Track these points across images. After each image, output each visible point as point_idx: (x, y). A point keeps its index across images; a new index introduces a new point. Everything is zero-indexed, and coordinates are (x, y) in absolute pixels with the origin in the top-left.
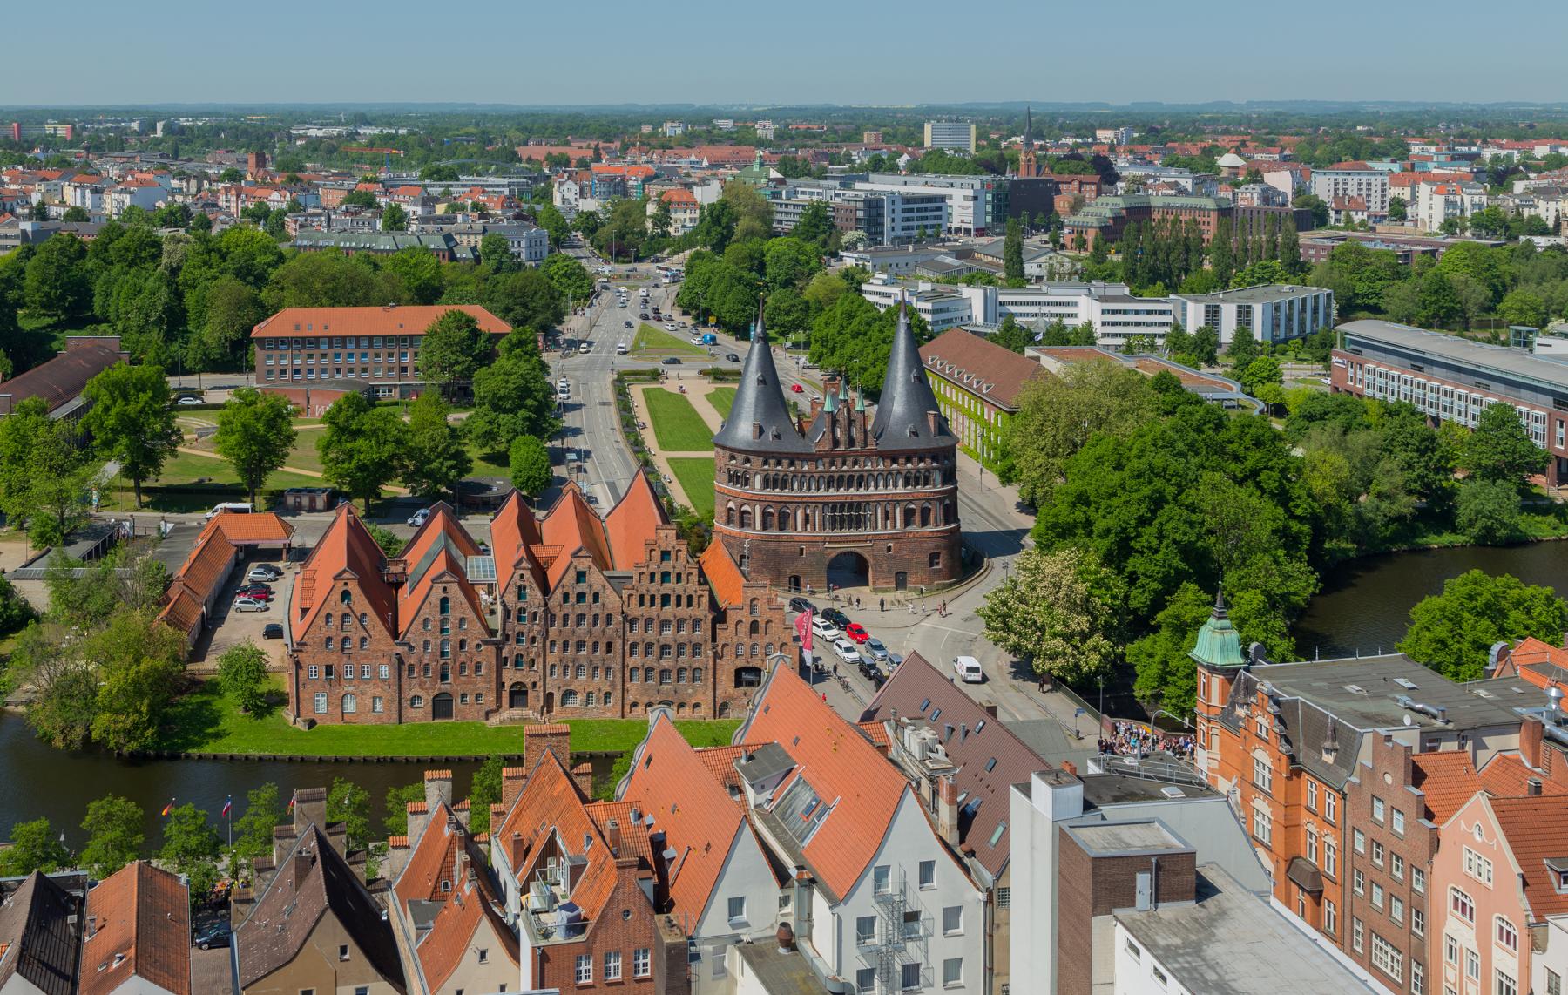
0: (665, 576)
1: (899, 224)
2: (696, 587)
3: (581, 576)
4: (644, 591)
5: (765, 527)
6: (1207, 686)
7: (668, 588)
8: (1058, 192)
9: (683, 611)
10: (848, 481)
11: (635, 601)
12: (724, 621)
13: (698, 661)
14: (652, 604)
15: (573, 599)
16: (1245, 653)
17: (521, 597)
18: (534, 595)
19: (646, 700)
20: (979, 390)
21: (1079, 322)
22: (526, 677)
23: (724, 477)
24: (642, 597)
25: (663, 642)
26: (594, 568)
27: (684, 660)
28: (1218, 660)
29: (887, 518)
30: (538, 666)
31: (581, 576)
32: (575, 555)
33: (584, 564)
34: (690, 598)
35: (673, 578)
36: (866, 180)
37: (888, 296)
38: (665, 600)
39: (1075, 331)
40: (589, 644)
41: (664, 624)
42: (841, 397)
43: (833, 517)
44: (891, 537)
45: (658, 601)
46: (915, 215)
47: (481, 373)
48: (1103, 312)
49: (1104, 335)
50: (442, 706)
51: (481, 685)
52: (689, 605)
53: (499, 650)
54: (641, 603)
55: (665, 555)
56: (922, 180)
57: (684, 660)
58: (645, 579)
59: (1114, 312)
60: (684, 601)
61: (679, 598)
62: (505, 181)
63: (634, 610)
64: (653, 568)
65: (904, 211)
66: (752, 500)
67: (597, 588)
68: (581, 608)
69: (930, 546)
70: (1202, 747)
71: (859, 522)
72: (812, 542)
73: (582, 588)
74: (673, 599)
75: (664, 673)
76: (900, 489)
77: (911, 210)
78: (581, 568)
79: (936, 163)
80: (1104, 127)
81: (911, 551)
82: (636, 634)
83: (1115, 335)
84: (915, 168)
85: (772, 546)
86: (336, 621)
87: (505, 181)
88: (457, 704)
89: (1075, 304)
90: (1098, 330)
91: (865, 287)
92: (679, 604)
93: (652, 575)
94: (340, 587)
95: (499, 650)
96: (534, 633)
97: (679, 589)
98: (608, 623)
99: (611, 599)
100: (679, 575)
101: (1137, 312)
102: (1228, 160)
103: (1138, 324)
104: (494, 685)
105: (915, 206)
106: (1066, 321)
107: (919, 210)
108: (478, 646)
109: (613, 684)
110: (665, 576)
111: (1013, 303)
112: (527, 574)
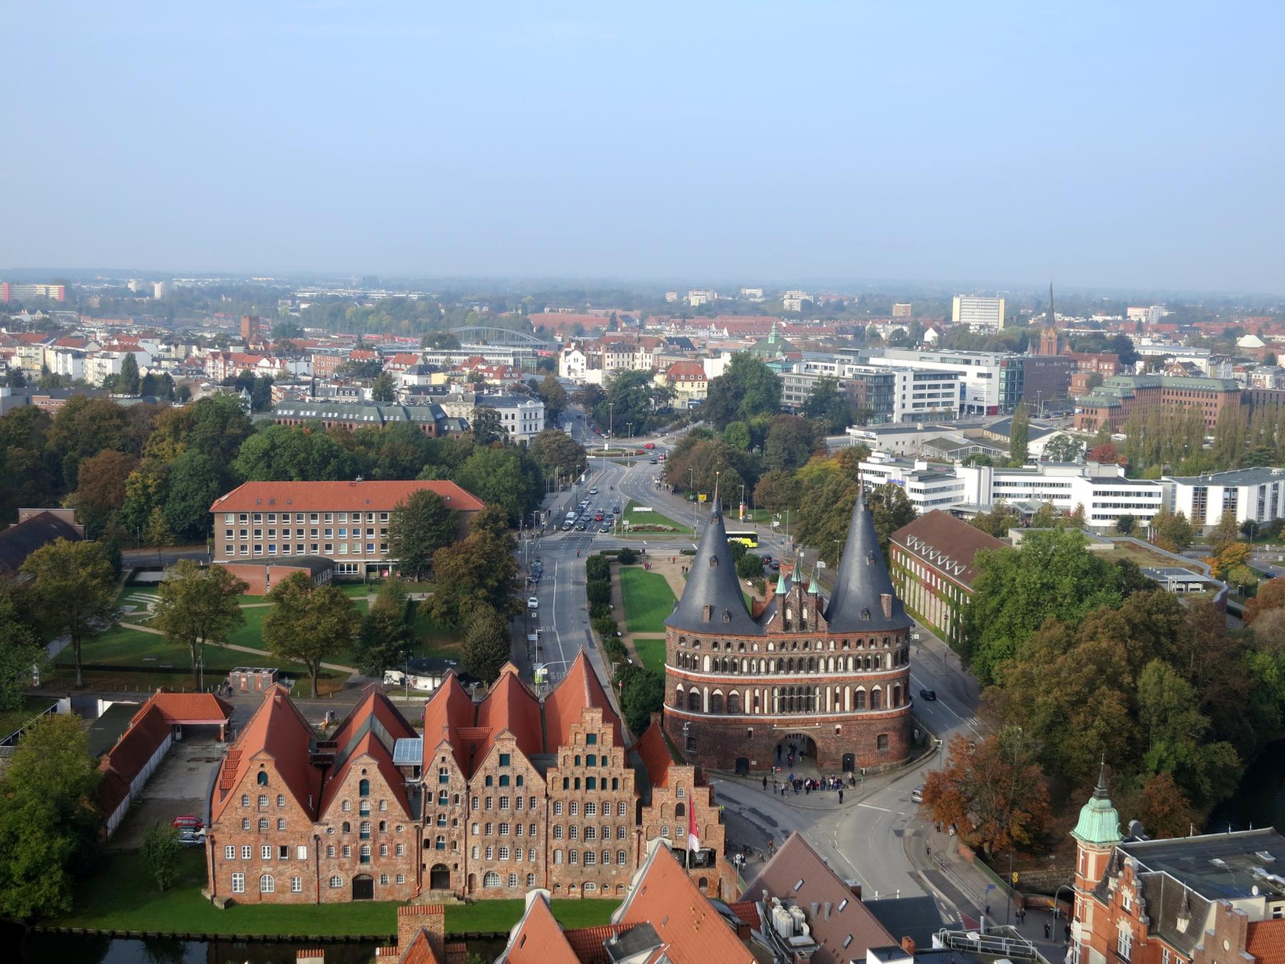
0: (591, 760)
1: (910, 401)
2: (622, 769)
3: (504, 760)
4: (568, 774)
5: (712, 711)
6: (1085, 862)
8: (1076, 369)
9: (608, 794)
10: (799, 665)
11: (560, 783)
12: (650, 804)
13: (622, 844)
14: (577, 786)
15: (496, 782)
16: (1123, 829)
17: (443, 780)
18: (457, 777)
19: (569, 881)
20: (951, 571)
21: (1072, 505)
23: (674, 660)
25: (586, 824)
26: (518, 752)
27: (607, 843)
28: (1096, 837)
29: (836, 701)
30: (461, 846)
31: (504, 760)
34: (615, 781)
35: (599, 761)
36: (882, 355)
37: (881, 474)
38: (590, 783)
39: (1066, 512)
40: (511, 827)
41: (588, 807)
42: (794, 579)
43: (782, 702)
44: (839, 720)
45: (583, 783)
46: (927, 391)
47: (442, 552)
48: (1096, 493)
49: (1095, 517)
50: (362, 887)
52: (615, 787)
53: (419, 831)
55: (591, 739)
56: (937, 356)
58: (571, 762)
59: (1105, 494)
60: (609, 784)
61: (604, 781)
62: (512, 350)
63: (558, 792)
64: (578, 751)
65: (915, 387)
66: (700, 683)
67: (520, 771)
68: (504, 791)
69: (880, 727)
70: (1078, 920)
71: (808, 705)
72: (761, 725)
75: (587, 856)
76: (851, 673)
77: (923, 387)
78: (504, 751)
79: (963, 341)
80: (1136, 304)
81: (859, 734)
82: (559, 818)
83: (1104, 517)
84: (941, 344)
85: (720, 729)
86: (251, 803)
87: (512, 350)
88: (377, 884)
89: (1069, 485)
90: (1089, 512)
91: (861, 466)
92: (604, 787)
93: (577, 759)
95: (419, 831)
96: (456, 815)
97: (604, 772)
98: (532, 805)
99: (534, 780)
101: (1139, 494)
102: (1249, 342)
103: (1139, 506)
104: (414, 866)
105: (941, 382)
106: (1057, 503)
107: (930, 387)
108: (398, 828)
110: (591, 760)
111: (1007, 484)
112: (450, 758)
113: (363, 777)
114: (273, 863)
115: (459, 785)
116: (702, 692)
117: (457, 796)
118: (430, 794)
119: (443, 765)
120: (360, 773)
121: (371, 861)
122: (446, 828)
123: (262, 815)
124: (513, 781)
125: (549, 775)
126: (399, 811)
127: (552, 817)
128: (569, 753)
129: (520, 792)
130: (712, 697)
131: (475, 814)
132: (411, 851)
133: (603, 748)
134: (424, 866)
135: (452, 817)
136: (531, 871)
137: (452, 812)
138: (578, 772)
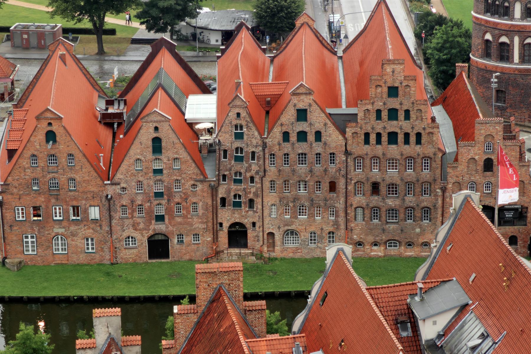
0: (393, 114)
4: (369, 129)
5: (523, 60)
7: (392, 126)
9: (412, 149)
13: (426, 200)
15: (293, 138)
17: (239, 136)
19: (371, 239)
22: (244, 216)
23: (482, 6)
24: (367, 135)
25: (388, 181)
26: (315, 107)
30: (258, 205)
32: (294, 94)
33: (303, 103)
34: (419, 136)
38: (393, 138)
41: (392, 162)
45: (385, 138)
50: (158, 248)
51: (198, 225)
52: (419, 141)
53: (214, 190)
54: (367, 141)
55: (393, 92)
57: (410, 200)
60: (413, 139)
61: (407, 136)
63: (359, 148)
64: (379, 105)
66: (510, 32)
67: (318, 126)
68: (302, 147)
73: (302, 126)
74: (401, 138)
75: (392, 212)
78: (301, 106)
92: (407, 141)
93: (379, 112)
94: (44, 127)
95: (214, 190)
96: (253, 173)
98: (332, 161)
99: (333, 137)
100: (407, 112)
104: (210, 224)
108: (194, 186)
109: (336, 223)
110: (393, 114)
113: (155, 135)
114: (65, 223)
115: (254, 142)
116: (512, 41)
117: (253, 153)
118: (225, 151)
119: (238, 122)
120: (152, 130)
121: (167, 220)
122: (243, 186)
123: (51, 175)
124: (311, 137)
125: (349, 131)
126: (192, 169)
127: (352, 174)
128: (370, 107)
129: (318, 148)
130: (523, 46)
131: (272, 170)
132: (207, 209)
133: (405, 102)
134: (221, 225)
135: (248, 175)
136: (331, 229)
137: (249, 169)
138: (379, 127)
